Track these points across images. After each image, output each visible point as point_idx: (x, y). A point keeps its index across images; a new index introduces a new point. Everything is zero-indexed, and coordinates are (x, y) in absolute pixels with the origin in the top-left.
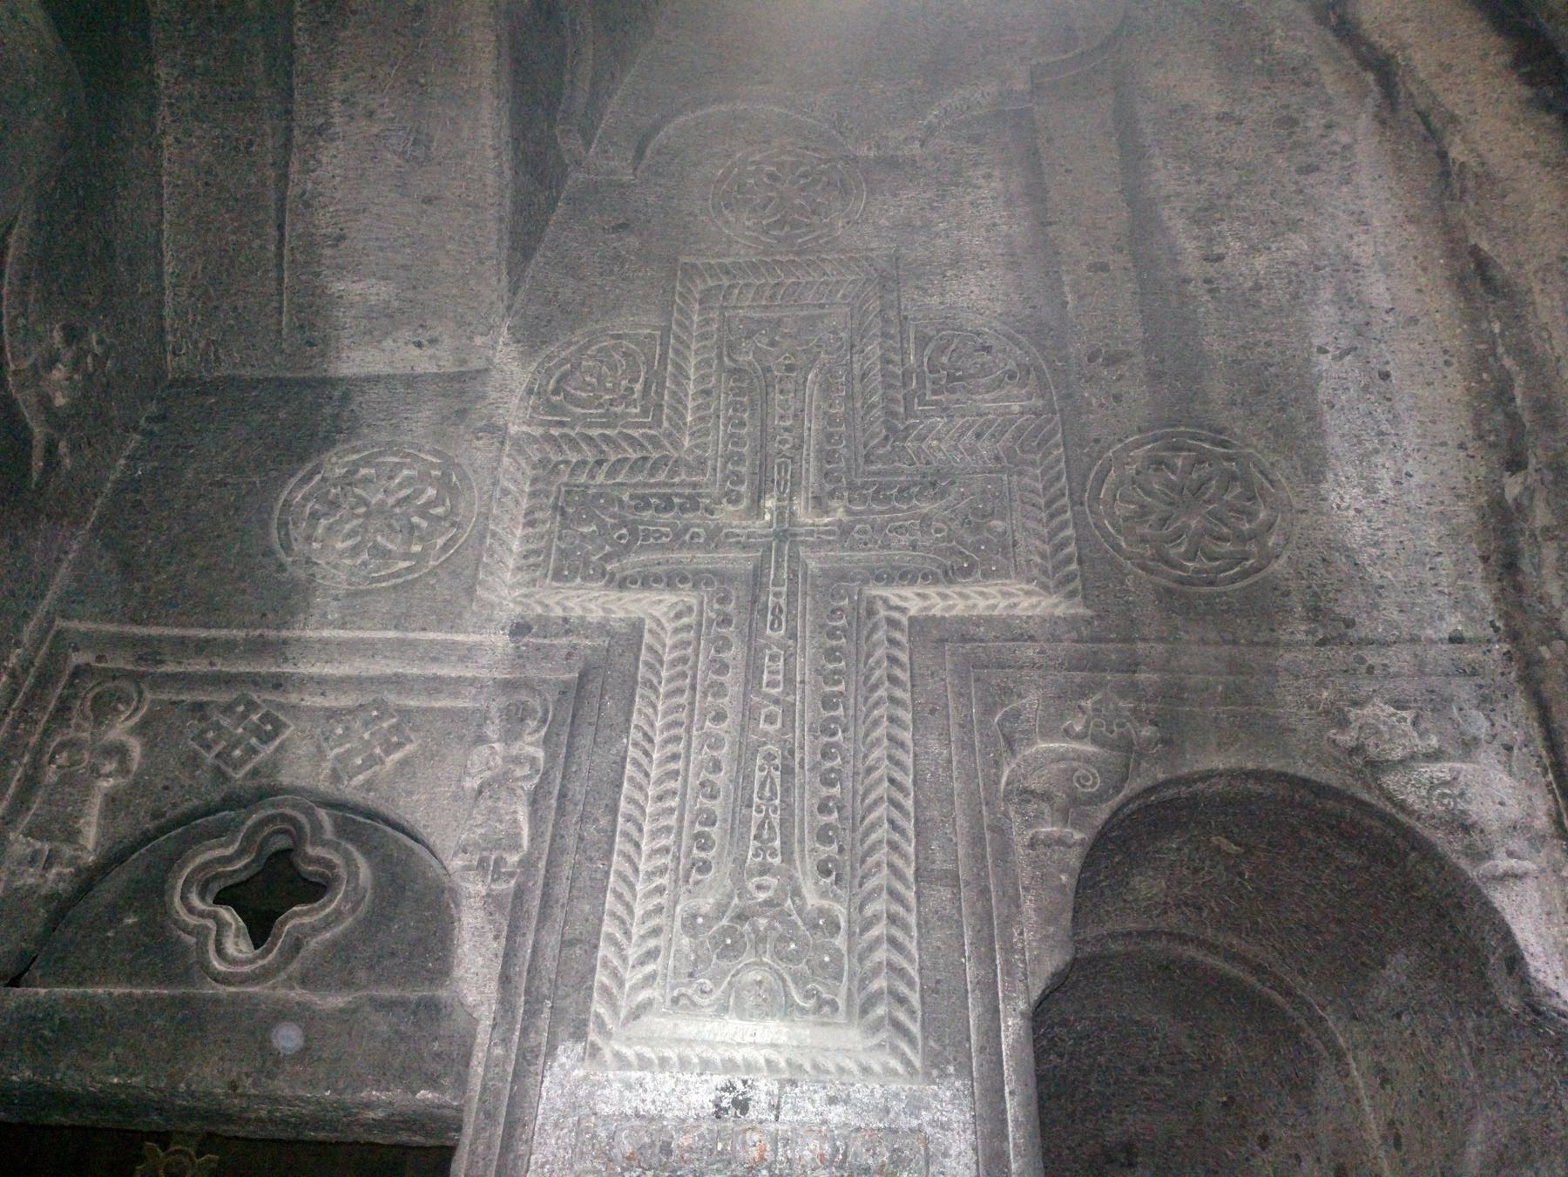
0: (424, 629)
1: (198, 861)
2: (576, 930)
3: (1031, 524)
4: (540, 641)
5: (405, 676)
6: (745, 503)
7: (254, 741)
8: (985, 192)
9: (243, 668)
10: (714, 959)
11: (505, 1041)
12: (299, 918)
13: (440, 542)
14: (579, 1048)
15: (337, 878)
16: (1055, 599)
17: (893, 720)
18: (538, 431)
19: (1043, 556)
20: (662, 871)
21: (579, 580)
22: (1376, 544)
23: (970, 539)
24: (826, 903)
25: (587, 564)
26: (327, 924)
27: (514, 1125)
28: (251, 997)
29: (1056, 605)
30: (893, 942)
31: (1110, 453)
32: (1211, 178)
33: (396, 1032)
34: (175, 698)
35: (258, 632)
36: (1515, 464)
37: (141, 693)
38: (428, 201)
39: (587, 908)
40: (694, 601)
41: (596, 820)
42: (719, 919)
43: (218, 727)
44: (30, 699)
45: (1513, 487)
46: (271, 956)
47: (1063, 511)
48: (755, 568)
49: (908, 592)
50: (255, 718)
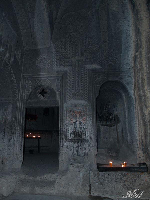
12: (45, 95)
13: (50, 64)
16: (99, 66)
17: (87, 78)
18: (56, 52)
20: (70, 90)
24: (82, 92)
27: (63, 108)
30: (87, 95)
36: (137, 52)
38: (43, 32)
45: (137, 54)
49: (88, 66)
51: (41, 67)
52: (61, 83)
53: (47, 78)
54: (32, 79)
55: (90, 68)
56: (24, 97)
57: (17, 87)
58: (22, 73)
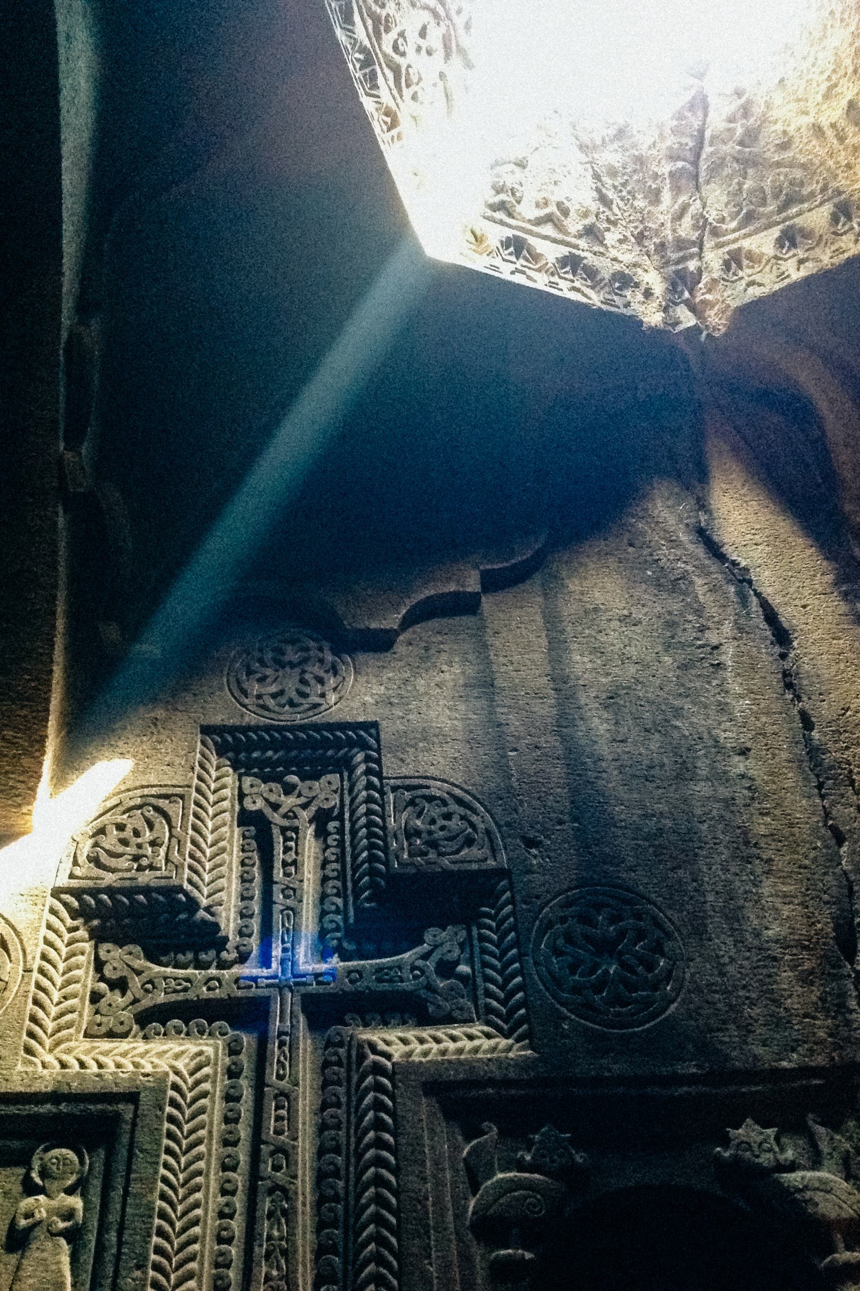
3: (489, 971)
6: (255, 952)
8: (447, 676)
16: (510, 1041)
19: (497, 999)
22: (744, 987)
23: (441, 984)
29: (509, 1049)
31: (546, 909)
32: (616, 670)
40: (209, 1051)
47: (512, 962)
49: (393, 1035)
55: (416, 1059)
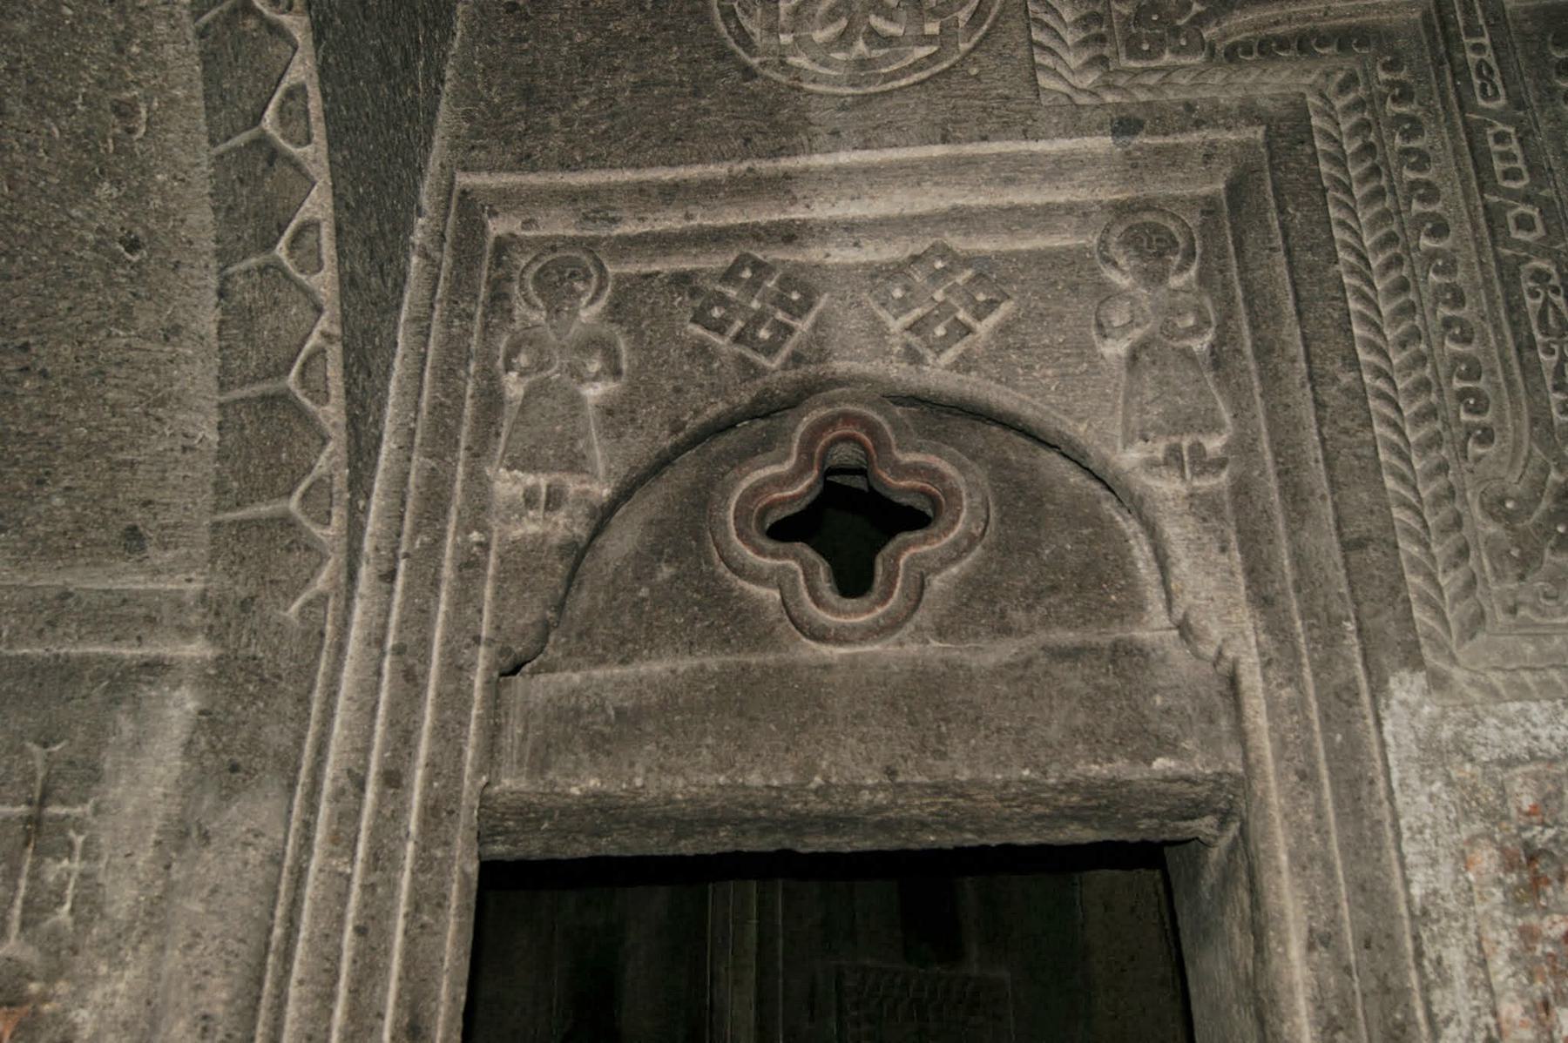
0: (985, 139)
1: (744, 484)
2: (1359, 526)
4: (1159, 141)
5: (970, 208)
7: (780, 315)
9: (731, 217)
10: (1547, 552)
11: (1294, 680)
13: (963, 15)
14: (1420, 679)
15: (952, 493)
21: (1167, 58)
25: (1176, 31)
26: (957, 552)
28: (875, 655)
33: (1098, 687)
34: (645, 270)
35: (745, 165)
37: (601, 268)
39: (1365, 496)
41: (1335, 380)
42: (1538, 500)
43: (723, 300)
44: (461, 286)
46: (891, 602)
48: (1426, 16)
50: (770, 284)
51: (801, 61)
52: (1227, 316)
53: (919, 247)
54: (631, 268)
56: (465, 596)
57: (335, 352)
58: (433, 165)
